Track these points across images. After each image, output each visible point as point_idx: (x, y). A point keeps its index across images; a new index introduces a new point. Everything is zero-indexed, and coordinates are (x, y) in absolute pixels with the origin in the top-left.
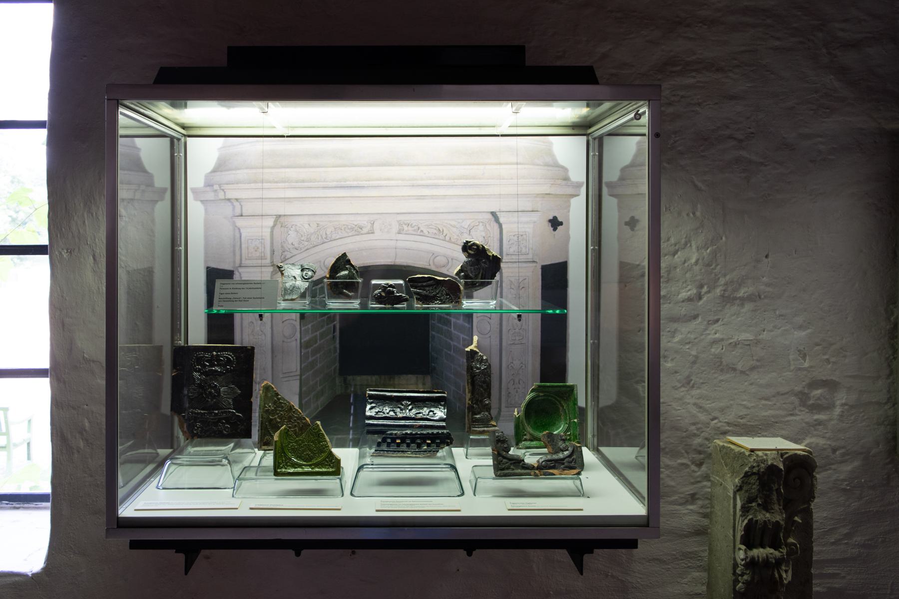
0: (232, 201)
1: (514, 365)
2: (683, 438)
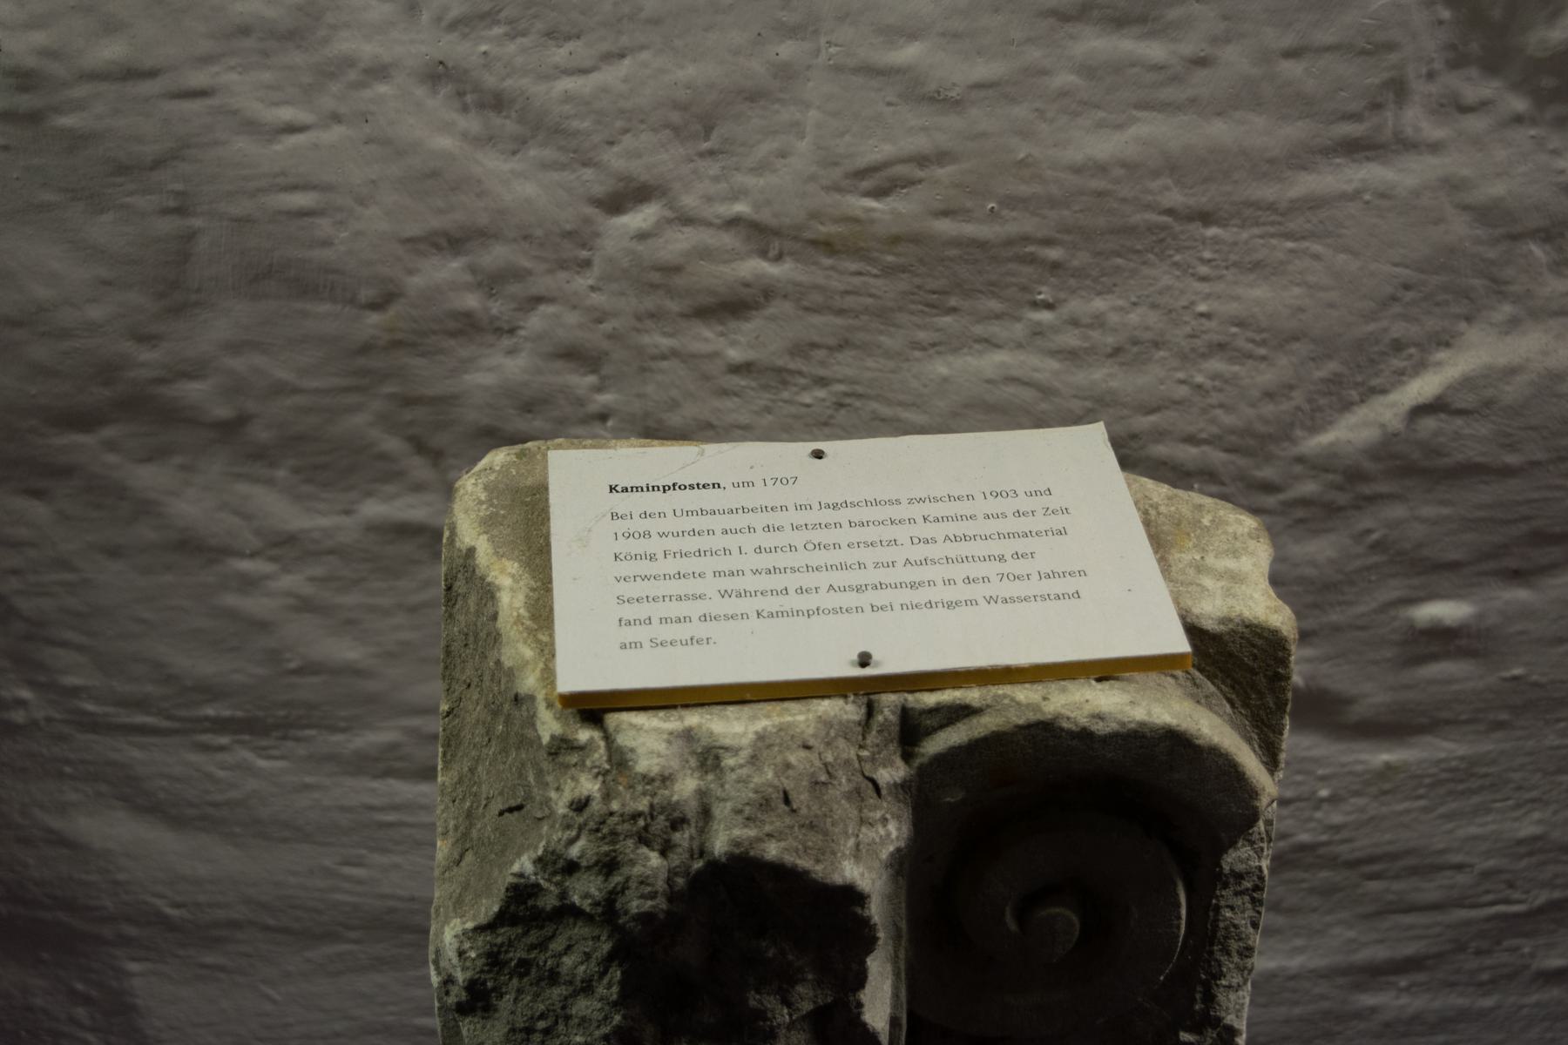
2: (366, 349)
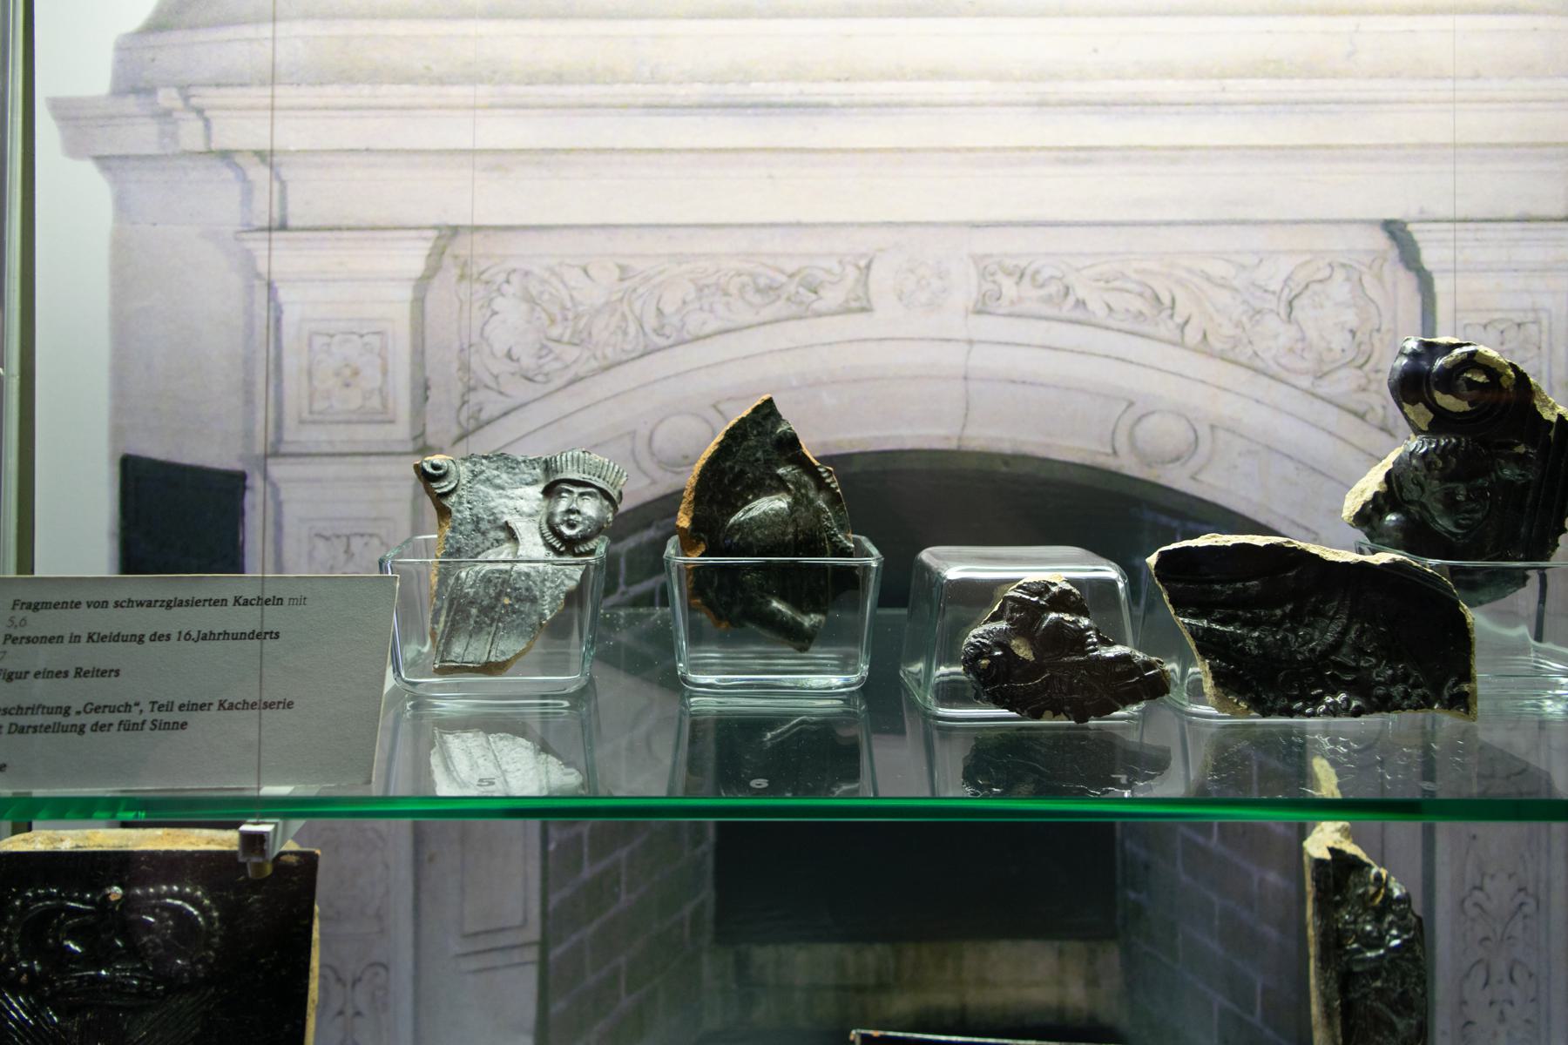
0: (238, 159)
1: (1489, 898)
